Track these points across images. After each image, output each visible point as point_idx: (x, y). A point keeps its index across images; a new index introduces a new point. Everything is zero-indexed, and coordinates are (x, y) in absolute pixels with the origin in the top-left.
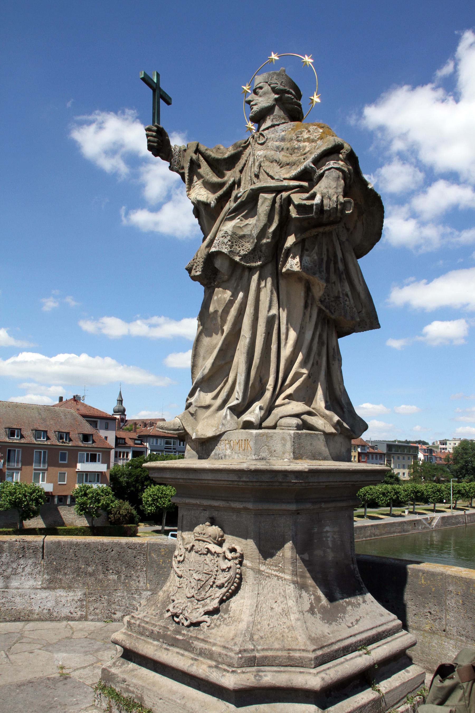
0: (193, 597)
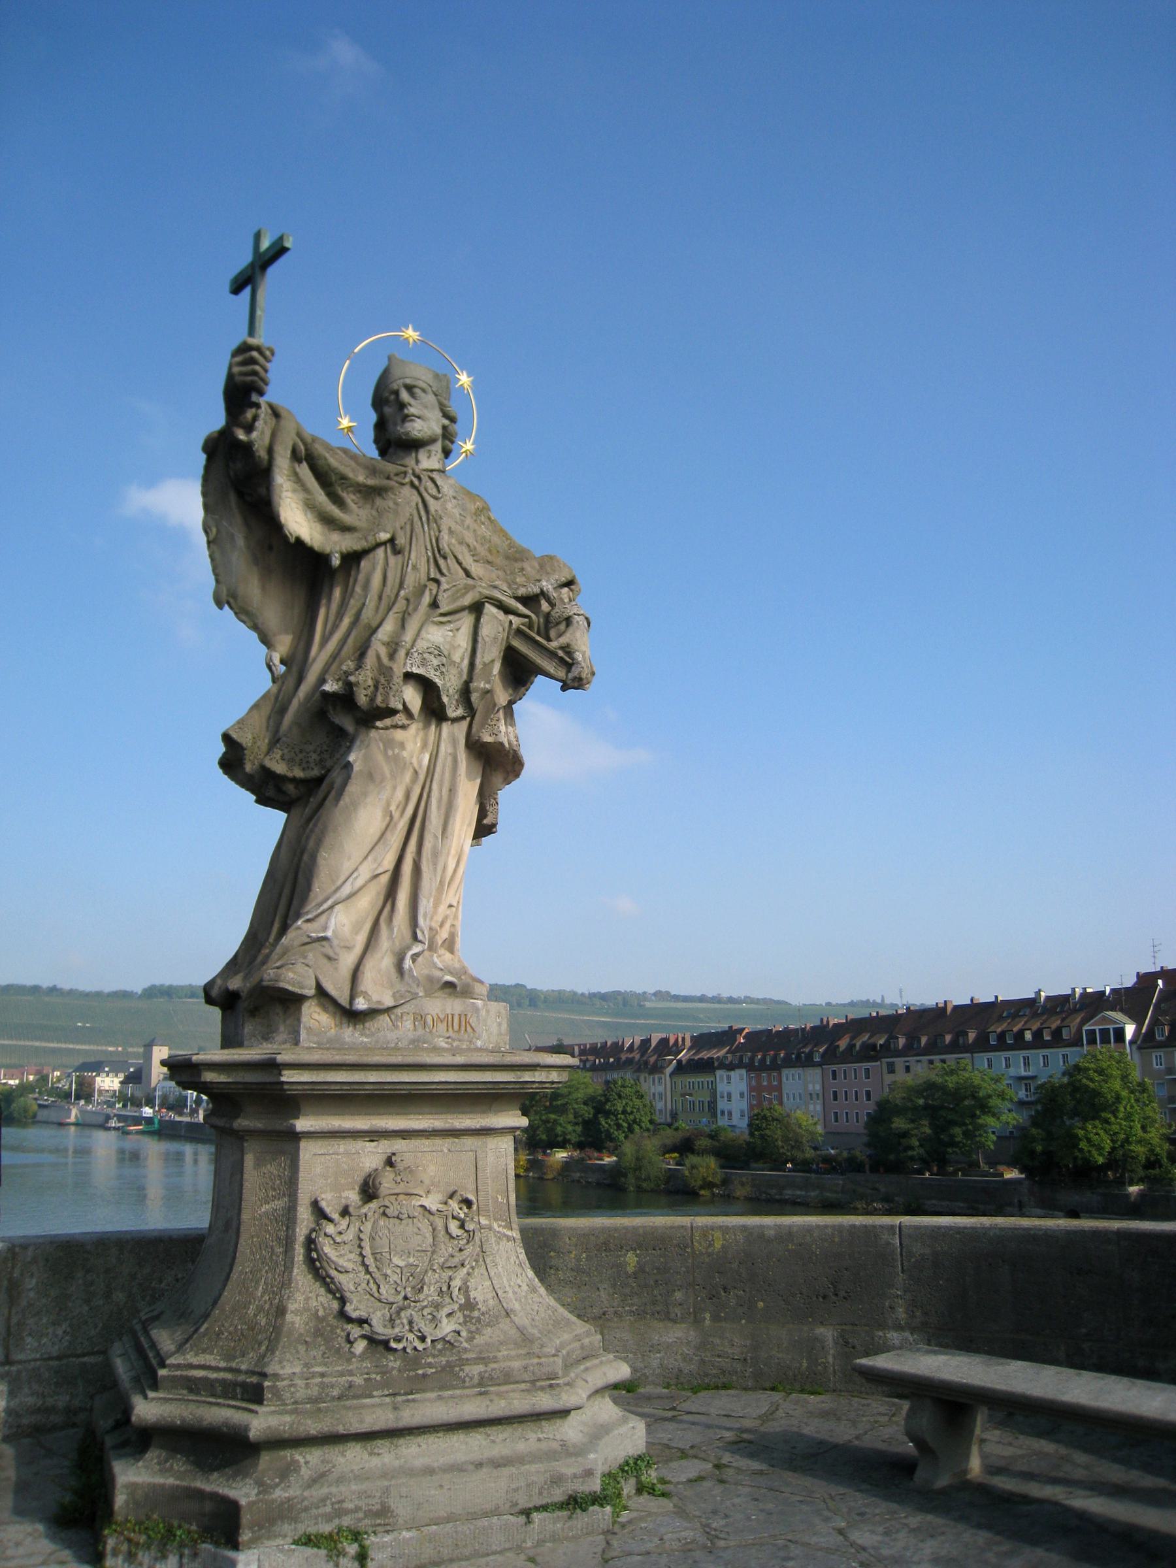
0: (406, 1298)
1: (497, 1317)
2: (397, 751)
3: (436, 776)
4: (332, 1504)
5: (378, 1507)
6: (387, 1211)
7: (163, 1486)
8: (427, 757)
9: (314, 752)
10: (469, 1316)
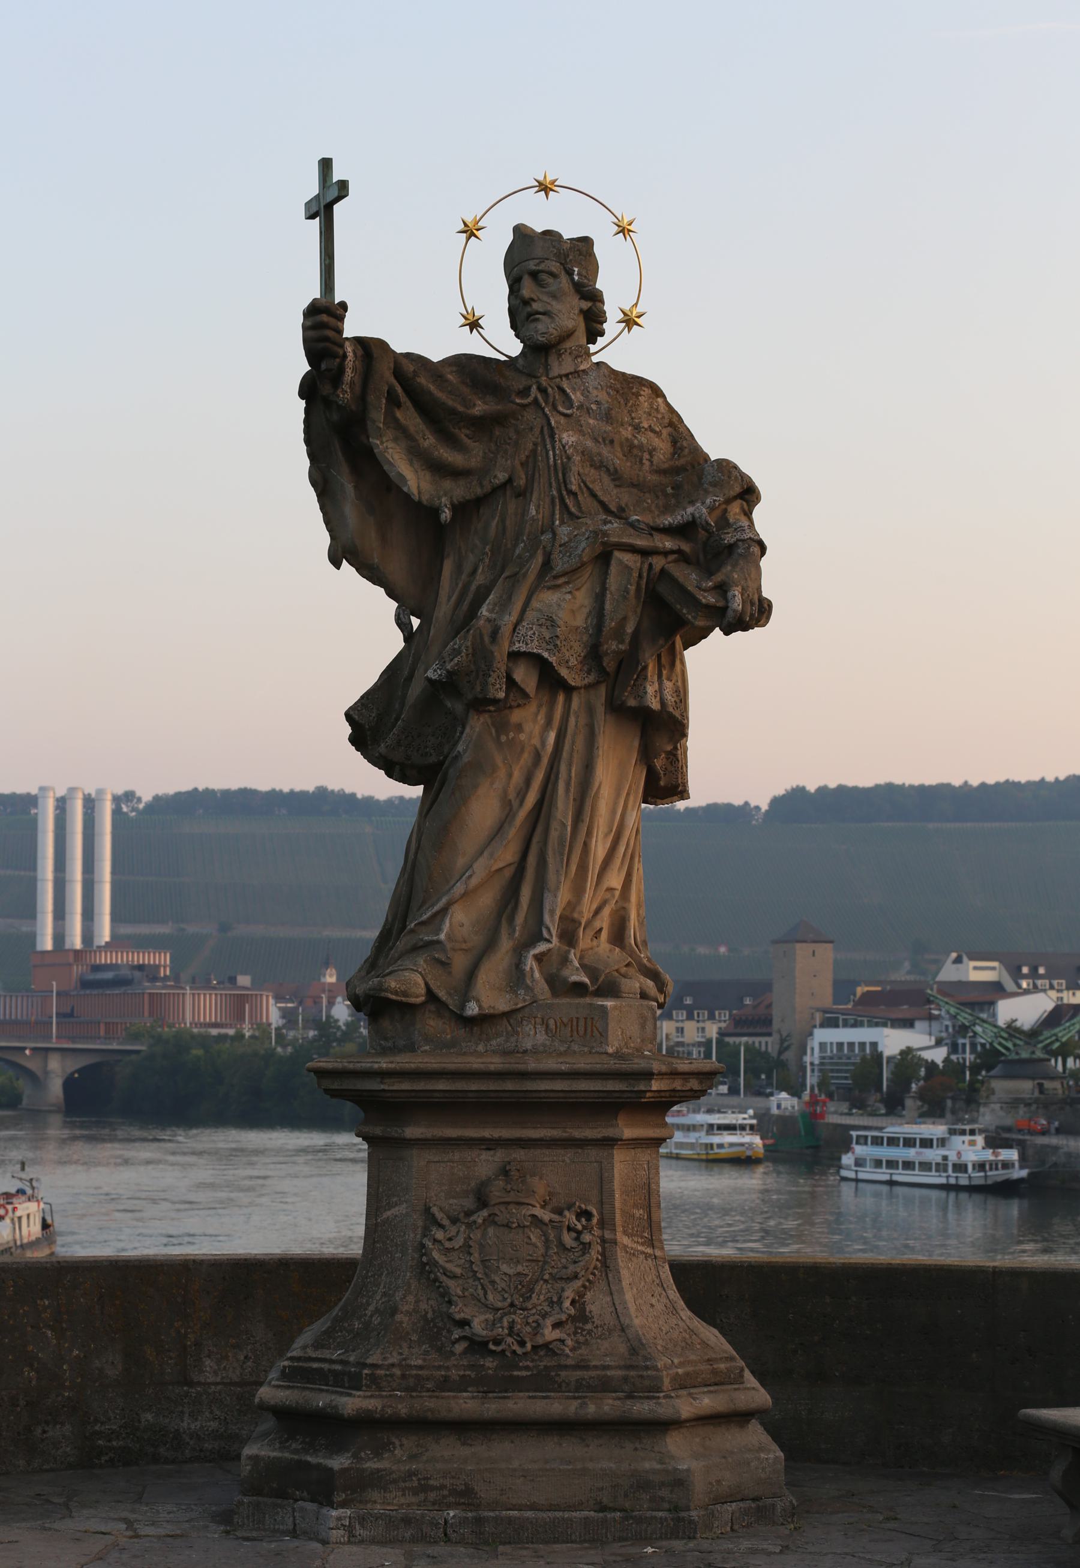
0: (512, 1305)
1: (610, 1331)
2: (511, 735)
3: (565, 755)
4: (419, 1480)
6: (497, 1219)
8: (552, 736)
9: (433, 736)
10: (580, 1328)
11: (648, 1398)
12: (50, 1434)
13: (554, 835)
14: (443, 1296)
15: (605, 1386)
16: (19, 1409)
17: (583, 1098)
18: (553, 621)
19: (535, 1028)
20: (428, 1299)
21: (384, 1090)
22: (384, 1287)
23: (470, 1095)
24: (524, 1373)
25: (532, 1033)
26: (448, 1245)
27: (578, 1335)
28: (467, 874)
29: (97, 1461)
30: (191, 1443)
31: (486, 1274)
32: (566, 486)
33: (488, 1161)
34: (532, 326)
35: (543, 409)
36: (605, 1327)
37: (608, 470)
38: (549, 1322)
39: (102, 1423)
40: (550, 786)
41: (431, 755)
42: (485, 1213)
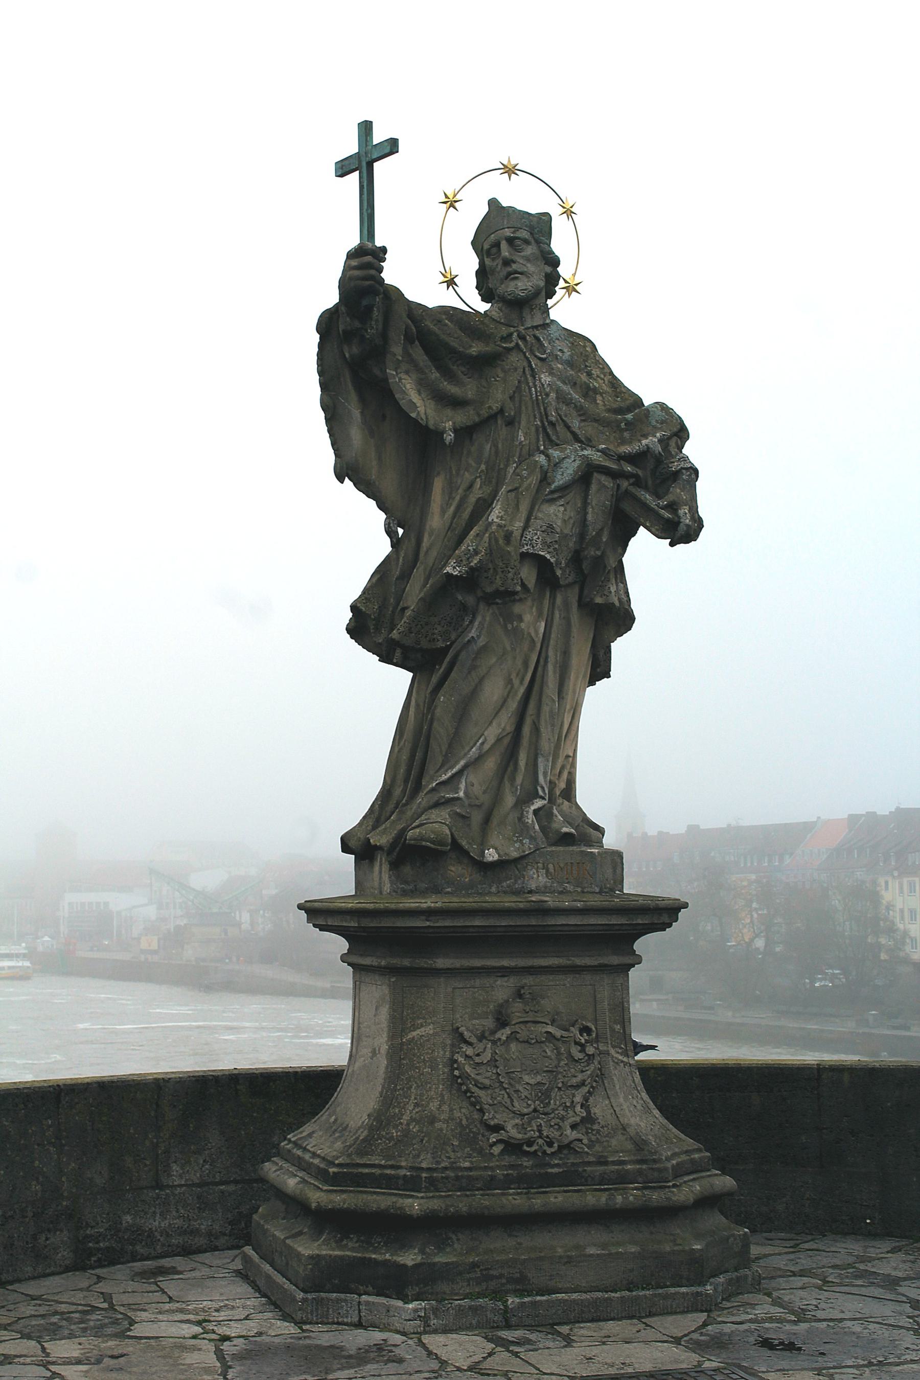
0: (535, 1110)
4: (481, 1270)
5: (518, 1275)
6: (518, 1036)
7: (341, 1258)
11: (661, 1187)
12: (52, 1240)
13: (546, 709)
14: (473, 1105)
15: (623, 1179)
16: (27, 1220)
17: (590, 931)
18: (553, 528)
19: (537, 872)
20: (460, 1108)
21: (429, 927)
22: (415, 1099)
23: (499, 929)
24: (555, 1170)
25: (535, 876)
26: (477, 1060)
27: (590, 1135)
28: (480, 741)
29: (88, 1262)
30: (162, 1239)
31: (510, 1084)
32: (547, 418)
33: (503, 986)
34: (512, 284)
35: (524, 354)
36: (610, 1127)
37: (576, 406)
38: (567, 1124)
39: (92, 1227)
40: (540, 669)
41: (438, 641)
42: (507, 1031)
